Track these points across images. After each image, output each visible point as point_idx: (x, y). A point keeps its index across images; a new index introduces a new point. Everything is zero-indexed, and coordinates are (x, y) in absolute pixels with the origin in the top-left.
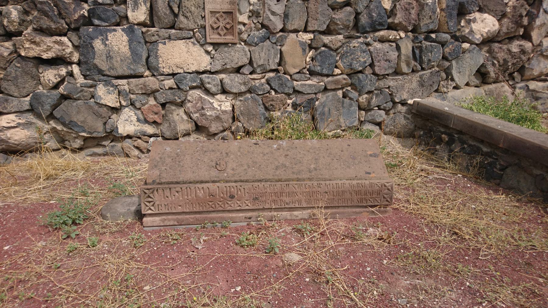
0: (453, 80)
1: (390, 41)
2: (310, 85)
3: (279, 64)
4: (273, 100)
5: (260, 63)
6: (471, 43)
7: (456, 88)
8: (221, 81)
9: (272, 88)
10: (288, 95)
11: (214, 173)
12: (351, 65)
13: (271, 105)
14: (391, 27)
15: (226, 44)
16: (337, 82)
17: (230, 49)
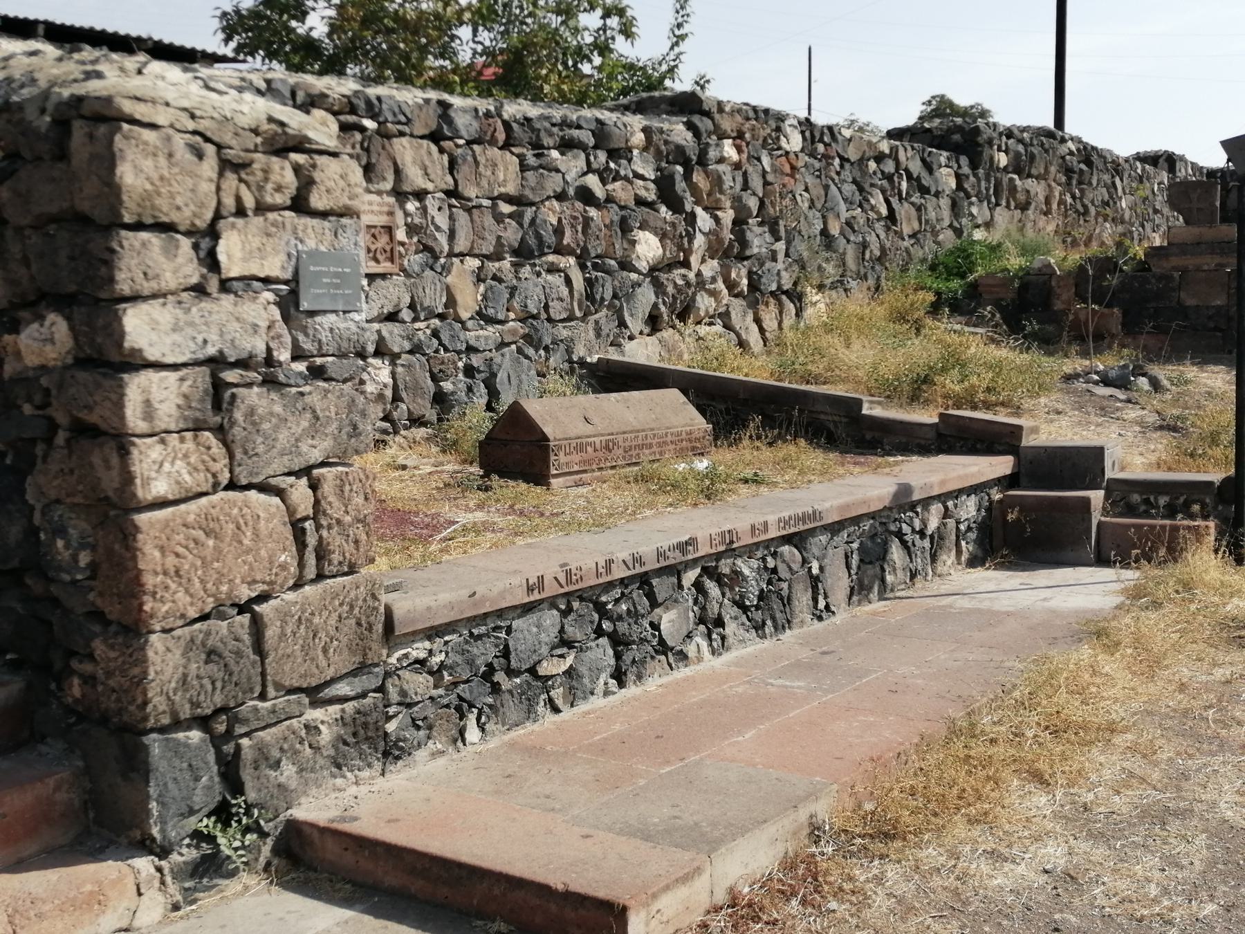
0: (626, 327)
1: (559, 271)
2: (486, 338)
3: (446, 306)
4: (443, 363)
5: (426, 305)
6: (640, 273)
7: (631, 338)
8: (379, 332)
9: (441, 344)
10: (459, 352)
11: (588, 429)
12: (526, 306)
13: (441, 371)
14: (559, 251)
15: (383, 276)
16: (513, 332)
17: (387, 282)
